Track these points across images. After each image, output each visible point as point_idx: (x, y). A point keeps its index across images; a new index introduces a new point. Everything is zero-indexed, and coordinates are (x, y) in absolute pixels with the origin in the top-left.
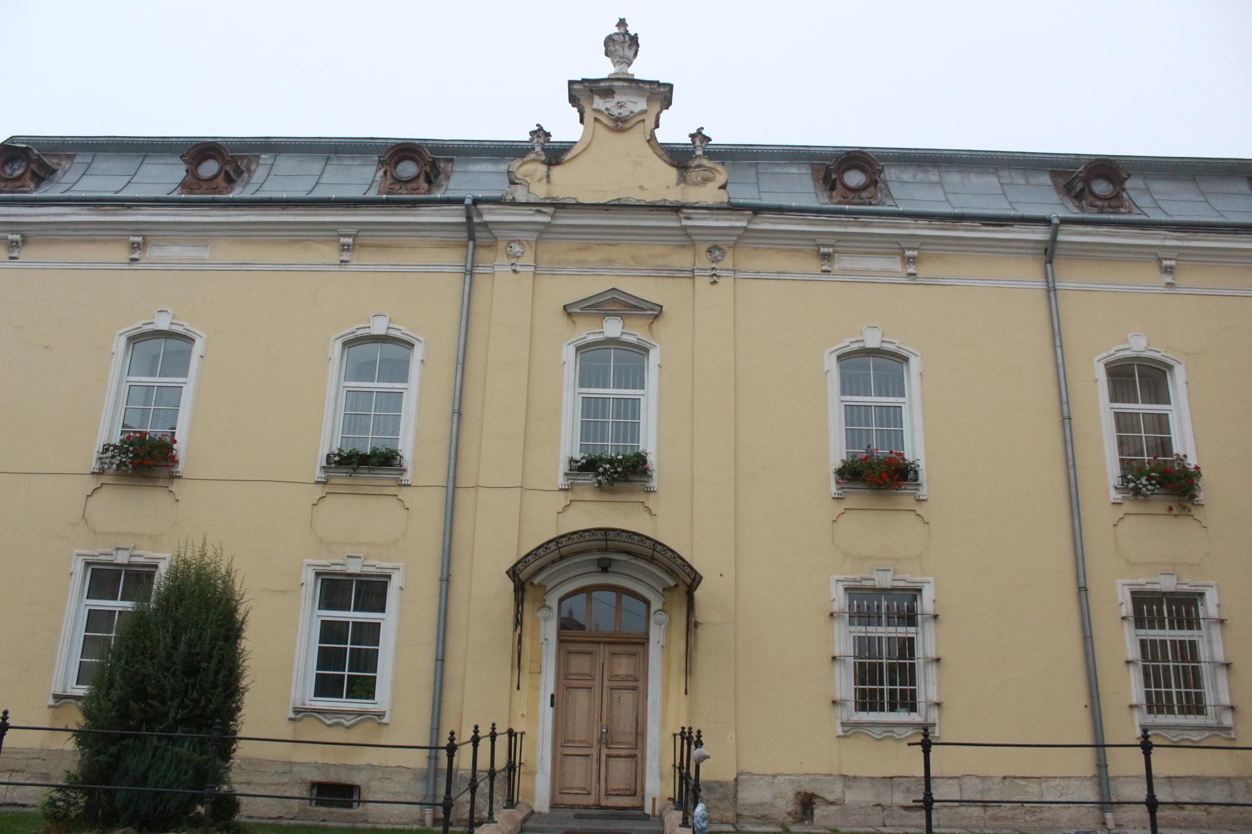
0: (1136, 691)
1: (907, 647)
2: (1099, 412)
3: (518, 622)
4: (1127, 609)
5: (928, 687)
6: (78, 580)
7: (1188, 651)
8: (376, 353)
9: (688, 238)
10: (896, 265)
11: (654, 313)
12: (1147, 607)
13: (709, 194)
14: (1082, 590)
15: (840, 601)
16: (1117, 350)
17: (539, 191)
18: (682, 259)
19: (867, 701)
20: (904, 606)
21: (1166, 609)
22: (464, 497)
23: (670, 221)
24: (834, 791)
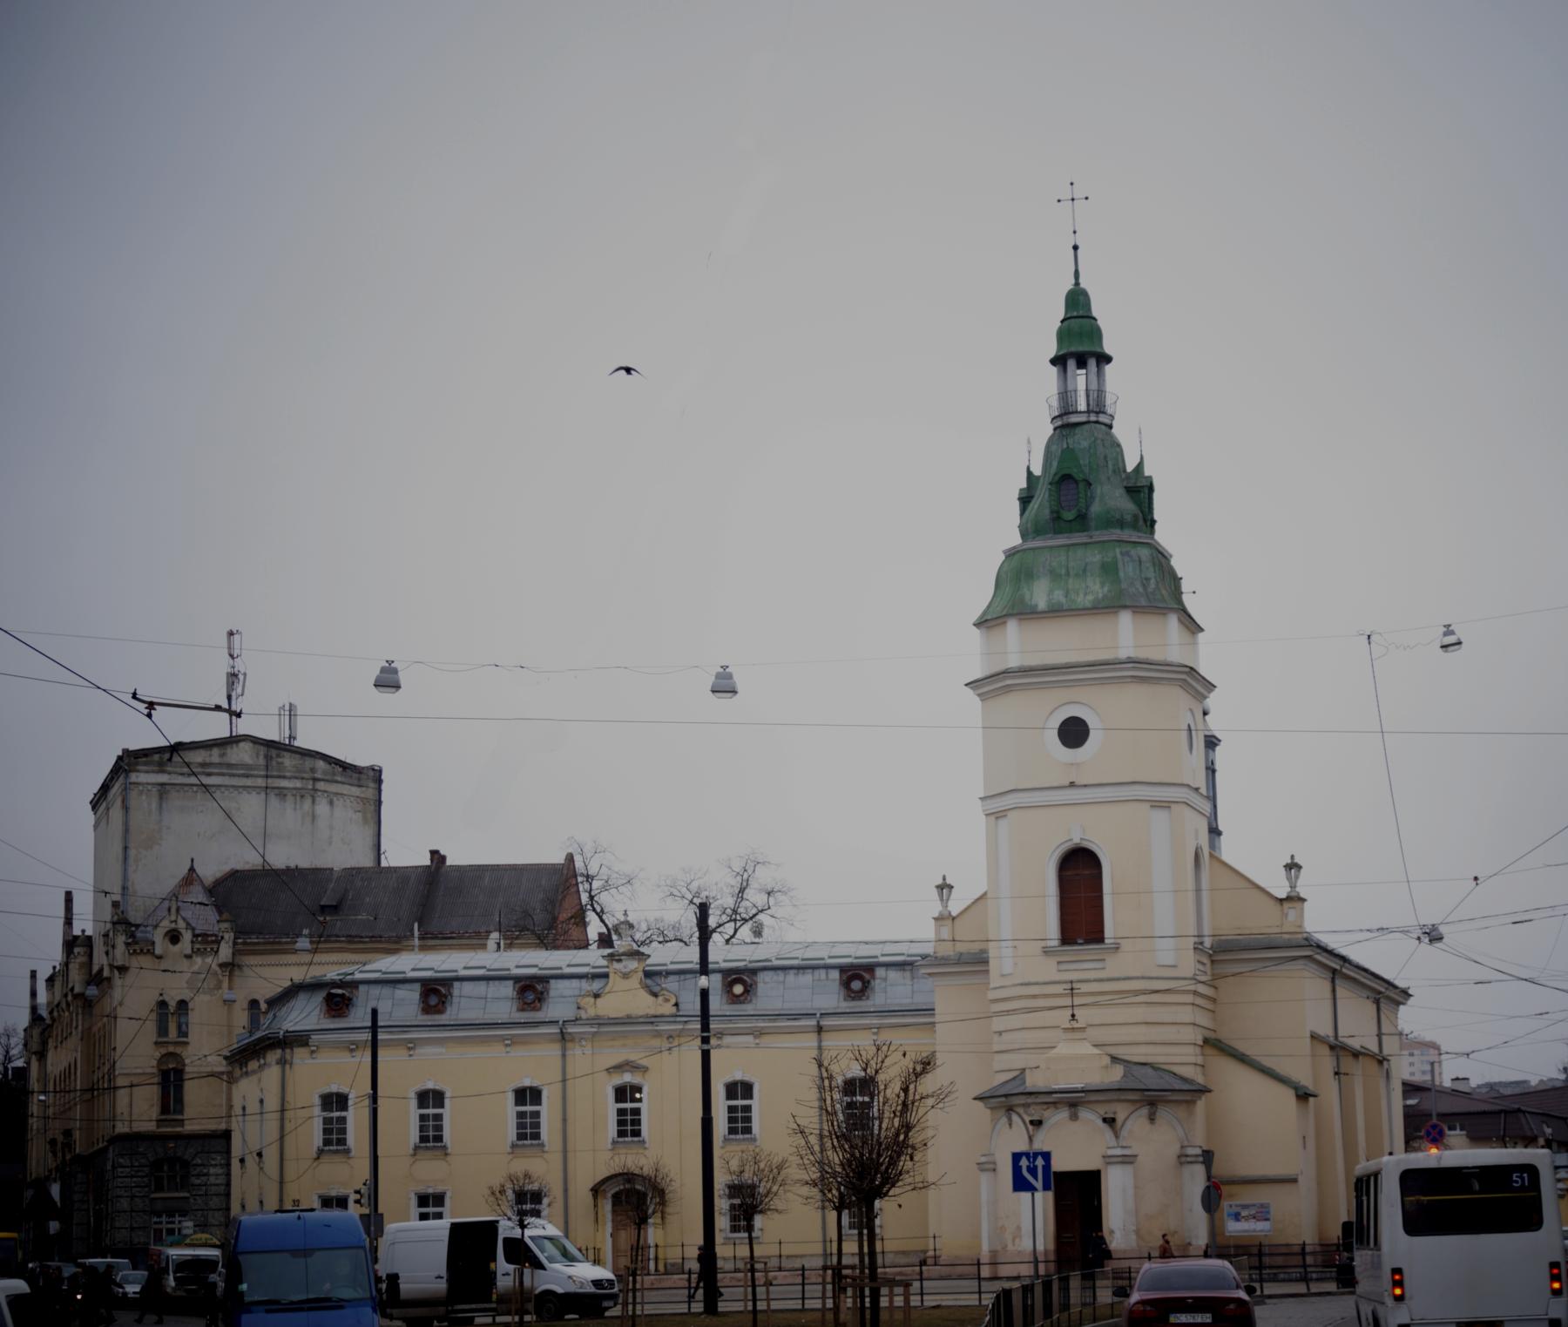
3: (596, 1206)
6: (414, 1201)
8: (530, 1095)
9: (658, 1034)
10: (750, 1038)
11: (645, 1069)
13: (668, 1009)
17: (592, 1012)
18: (656, 1042)
22: (570, 1155)
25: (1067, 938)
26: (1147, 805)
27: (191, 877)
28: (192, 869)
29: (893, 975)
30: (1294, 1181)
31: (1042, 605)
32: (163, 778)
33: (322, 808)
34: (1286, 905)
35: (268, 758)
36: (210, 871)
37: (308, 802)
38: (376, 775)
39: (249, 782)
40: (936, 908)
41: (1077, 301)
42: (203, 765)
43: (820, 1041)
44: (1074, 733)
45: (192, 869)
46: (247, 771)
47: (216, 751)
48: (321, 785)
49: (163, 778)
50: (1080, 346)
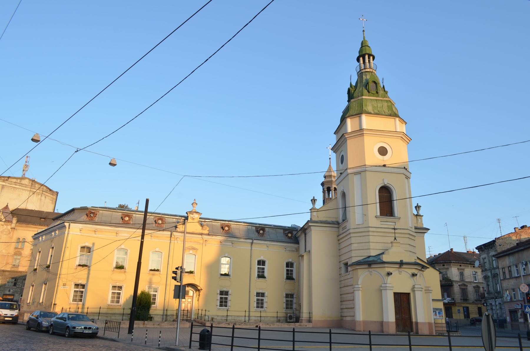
0: (255, 305)
1: (226, 298)
2: (256, 267)
4: (255, 294)
5: (229, 304)
7: (262, 300)
12: (258, 294)
13: (206, 232)
14: (250, 292)
15: (219, 292)
16: (259, 259)
19: (221, 306)
20: (227, 293)
21: (260, 295)
23: (200, 236)
24: (215, 317)
25: (382, 214)
26: (404, 176)
27: (7, 207)
28: (7, 205)
29: (271, 230)
30: (433, 300)
31: (372, 112)
32: (4, 184)
33: (43, 198)
34: (418, 217)
35: (32, 184)
36: (12, 208)
37: (40, 196)
38: (57, 193)
39: (26, 189)
40: (311, 206)
41: (363, 45)
42: (15, 182)
43: (251, 247)
44: (383, 151)
45: (7, 205)
46: (26, 186)
47: (19, 180)
48: (44, 193)
49: (4, 184)
50: (364, 54)
